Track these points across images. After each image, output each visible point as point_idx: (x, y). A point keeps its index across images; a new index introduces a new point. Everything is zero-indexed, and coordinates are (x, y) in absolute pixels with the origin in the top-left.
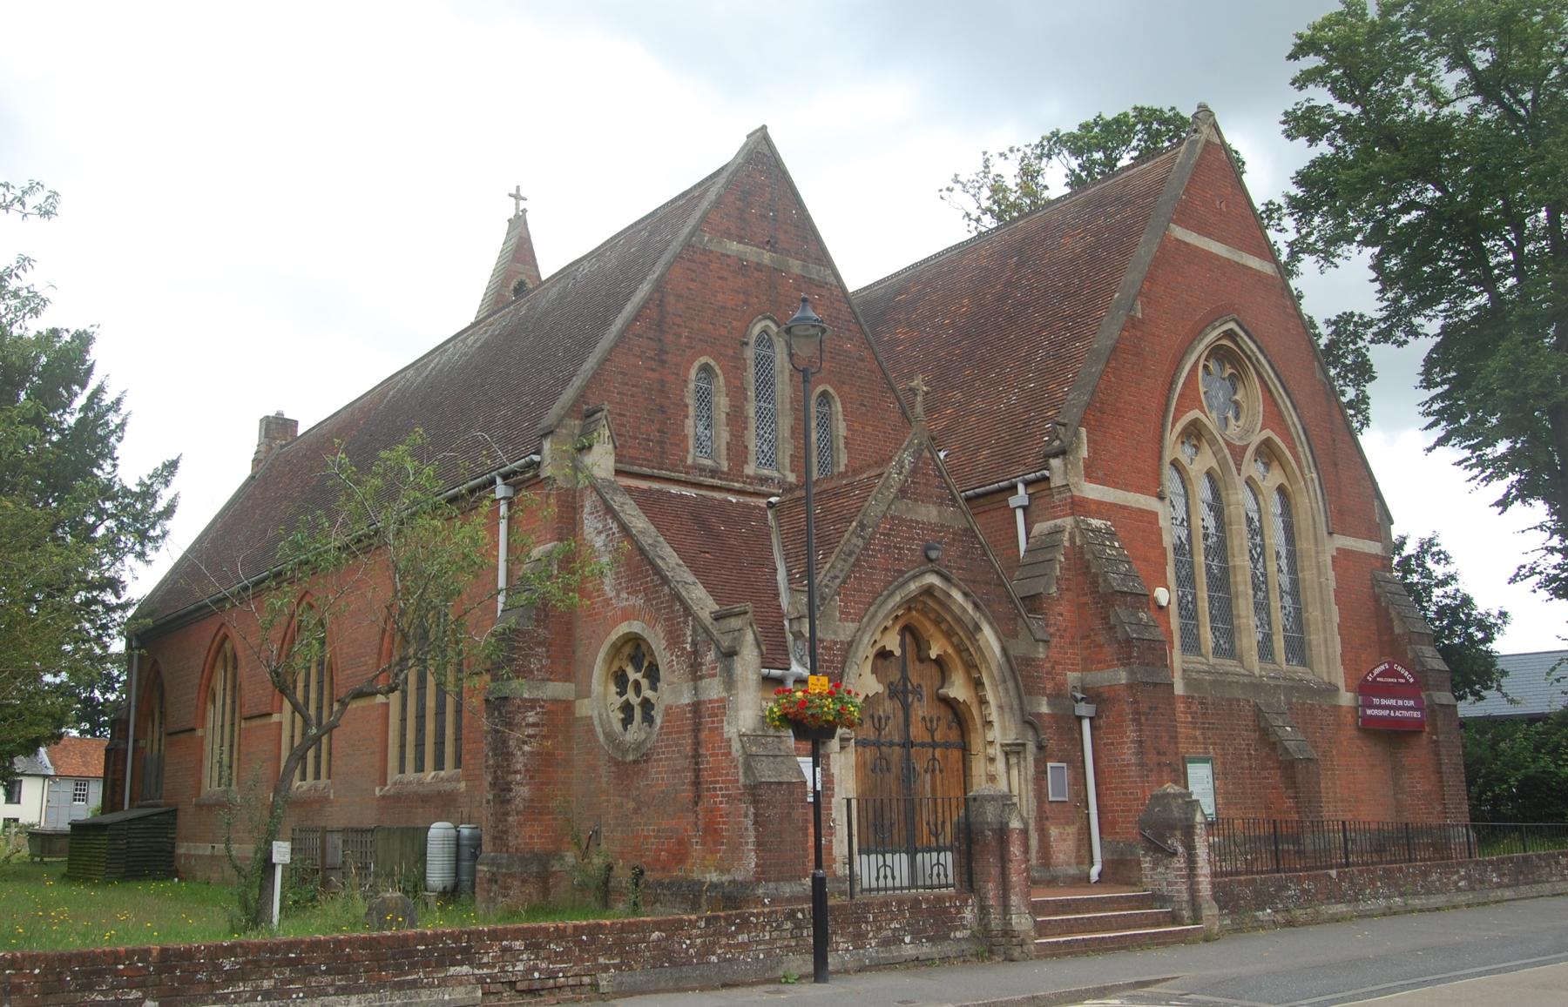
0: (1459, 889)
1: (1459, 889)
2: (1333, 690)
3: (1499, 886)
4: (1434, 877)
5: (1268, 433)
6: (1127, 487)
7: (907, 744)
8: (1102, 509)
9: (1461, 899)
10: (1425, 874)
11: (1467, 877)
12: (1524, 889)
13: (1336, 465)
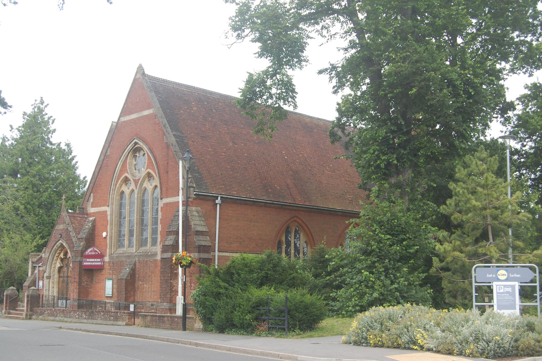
0: (76, 318)
1: (76, 318)
2: (155, 254)
3: (85, 318)
4: (72, 313)
5: (149, 170)
6: (100, 206)
7: (68, 277)
8: (94, 214)
9: (74, 320)
10: (70, 312)
11: (78, 315)
12: (90, 321)
13: (167, 172)
